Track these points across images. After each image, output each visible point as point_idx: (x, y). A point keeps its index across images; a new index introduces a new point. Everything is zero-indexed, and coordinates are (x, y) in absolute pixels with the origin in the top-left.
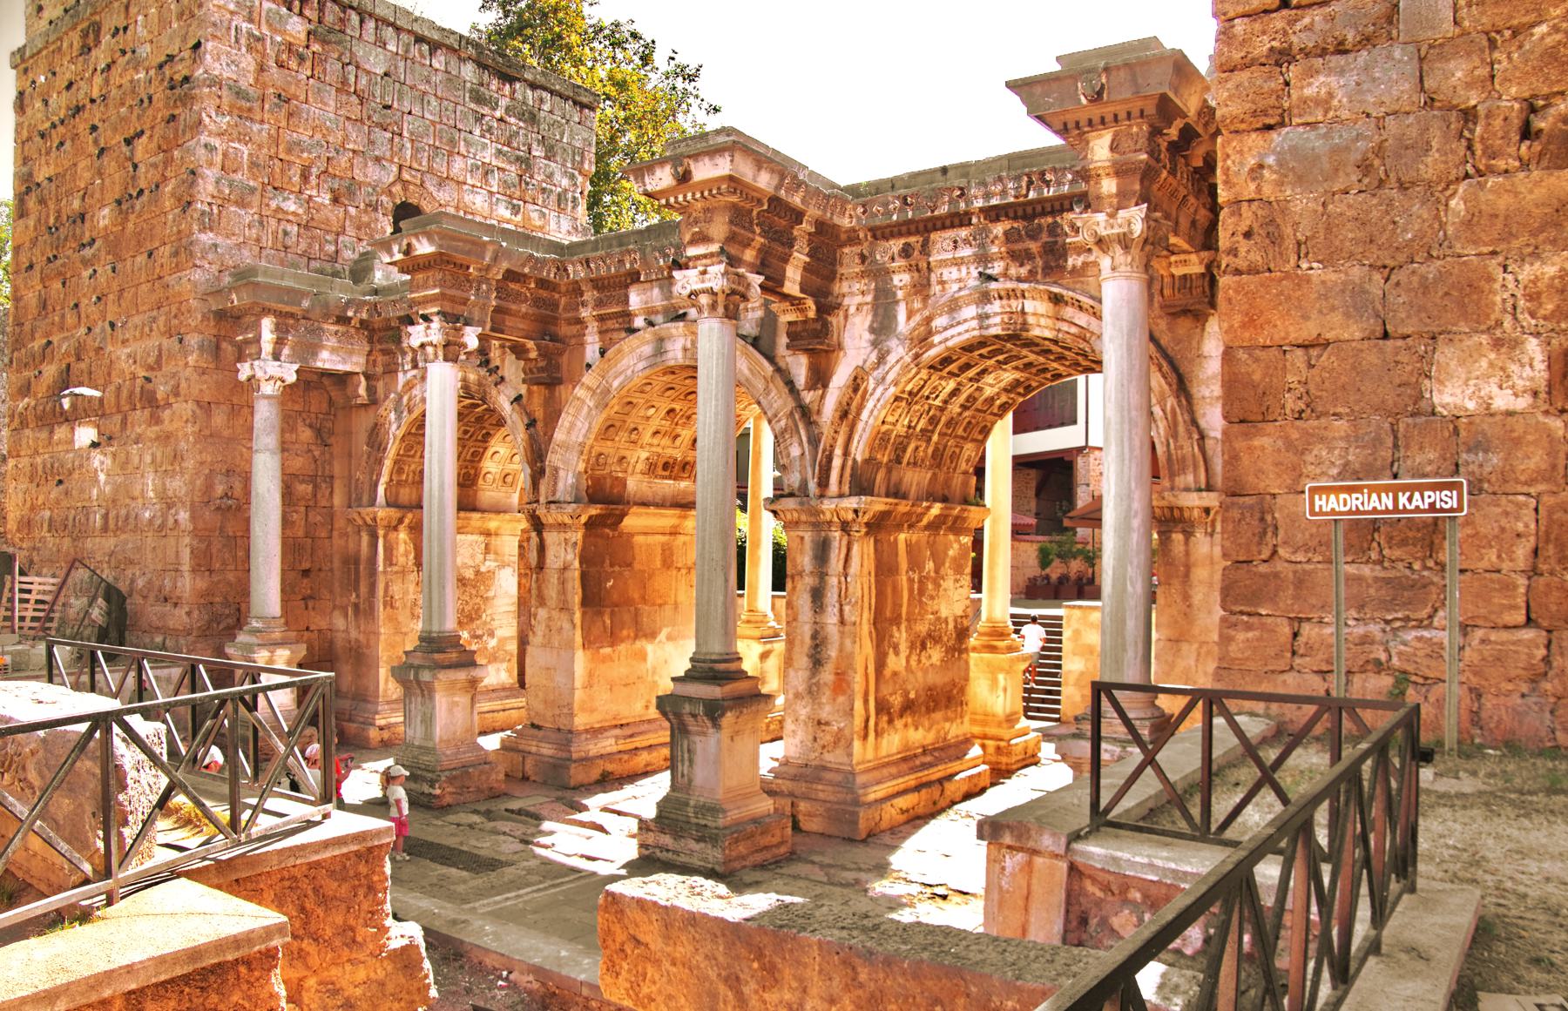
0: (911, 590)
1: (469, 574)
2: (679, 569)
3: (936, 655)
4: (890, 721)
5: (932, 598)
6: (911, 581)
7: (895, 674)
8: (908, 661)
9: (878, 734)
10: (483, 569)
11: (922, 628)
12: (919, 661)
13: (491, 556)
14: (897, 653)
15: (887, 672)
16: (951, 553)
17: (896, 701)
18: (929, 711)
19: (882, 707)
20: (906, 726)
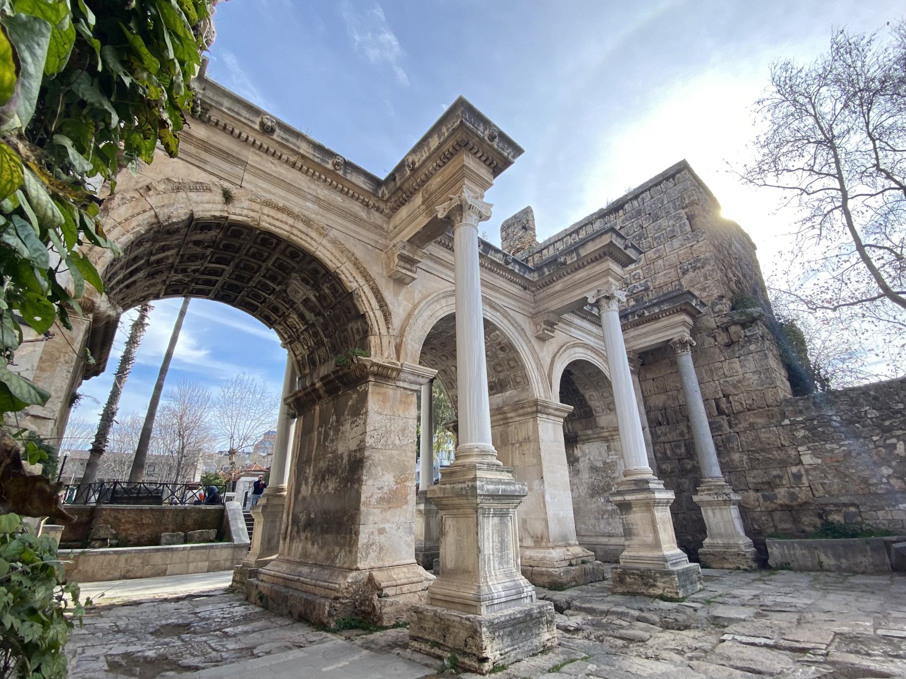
0: (319, 440)
1: (599, 464)
2: (513, 444)
3: (331, 485)
4: (298, 532)
5: (332, 441)
6: (319, 433)
7: (304, 498)
8: (312, 490)
9: (292, 539)
10: (608, 461)
11: (323, 465)
12: (319, 490)
13: (613, 452)
14: (306, 484)
15: (300, 497)
16: (350, 403)
17: (303, 518)
18: (324, 531)
19: (295, 521)
20: (306, 538)
